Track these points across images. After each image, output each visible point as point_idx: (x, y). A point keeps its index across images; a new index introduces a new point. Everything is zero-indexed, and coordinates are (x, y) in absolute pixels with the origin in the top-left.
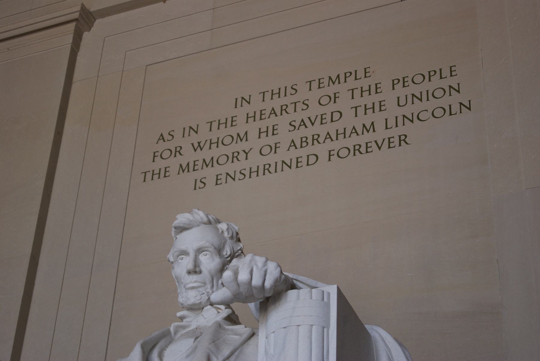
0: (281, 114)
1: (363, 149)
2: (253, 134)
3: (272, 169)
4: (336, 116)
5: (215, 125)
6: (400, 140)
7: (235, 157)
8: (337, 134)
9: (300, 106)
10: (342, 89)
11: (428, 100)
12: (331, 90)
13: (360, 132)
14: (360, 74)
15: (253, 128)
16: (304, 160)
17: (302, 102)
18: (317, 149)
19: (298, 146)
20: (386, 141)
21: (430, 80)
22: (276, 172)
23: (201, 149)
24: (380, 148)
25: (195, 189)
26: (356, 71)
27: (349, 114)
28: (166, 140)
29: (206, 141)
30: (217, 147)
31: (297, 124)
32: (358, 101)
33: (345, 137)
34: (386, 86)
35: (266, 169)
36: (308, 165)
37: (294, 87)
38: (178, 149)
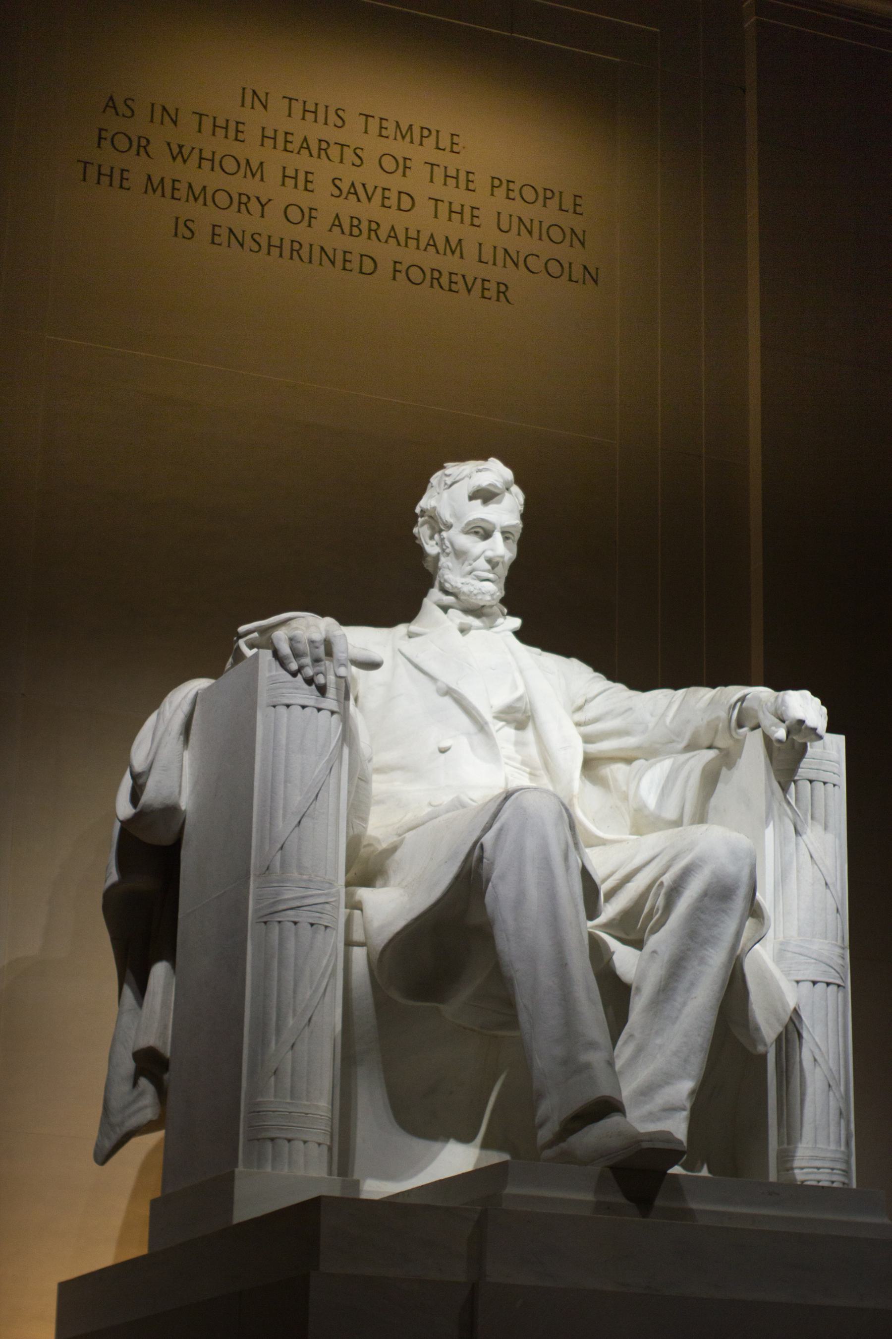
0: (319, 157)
1: (445, 281)
2: (273, 173)
3: (305, 253)
4: (406, 202)
5: (207, 123)
6: (499, 292)
7: (242, 202)
8: (407, 238)
9: (348, 152)
10: (420, 155)
11: (540, 239)
12: (401, 148)
13: (441, 251)
14: (445, 142)
15: (275, 160)
16: (355, 259)
17: (352, 148)
18: (374, 248)
19: (347, 229)
20: (479, 282)
21: (545, 206)
22: (310, 262)
23: (185, 161)
24: (469, 291)
25: (176, 235)
26: (438, 132)
27: (425, 208)
28: (120, 113)
29: (193, 148)
30: (212, 169)
31: (345, 186)
32: (436, 189)
33: (418, 248)
34: (481, 182)
35: (296, 248)
36: (361, 272)
37: (340, 112)
38: (143, 142)
